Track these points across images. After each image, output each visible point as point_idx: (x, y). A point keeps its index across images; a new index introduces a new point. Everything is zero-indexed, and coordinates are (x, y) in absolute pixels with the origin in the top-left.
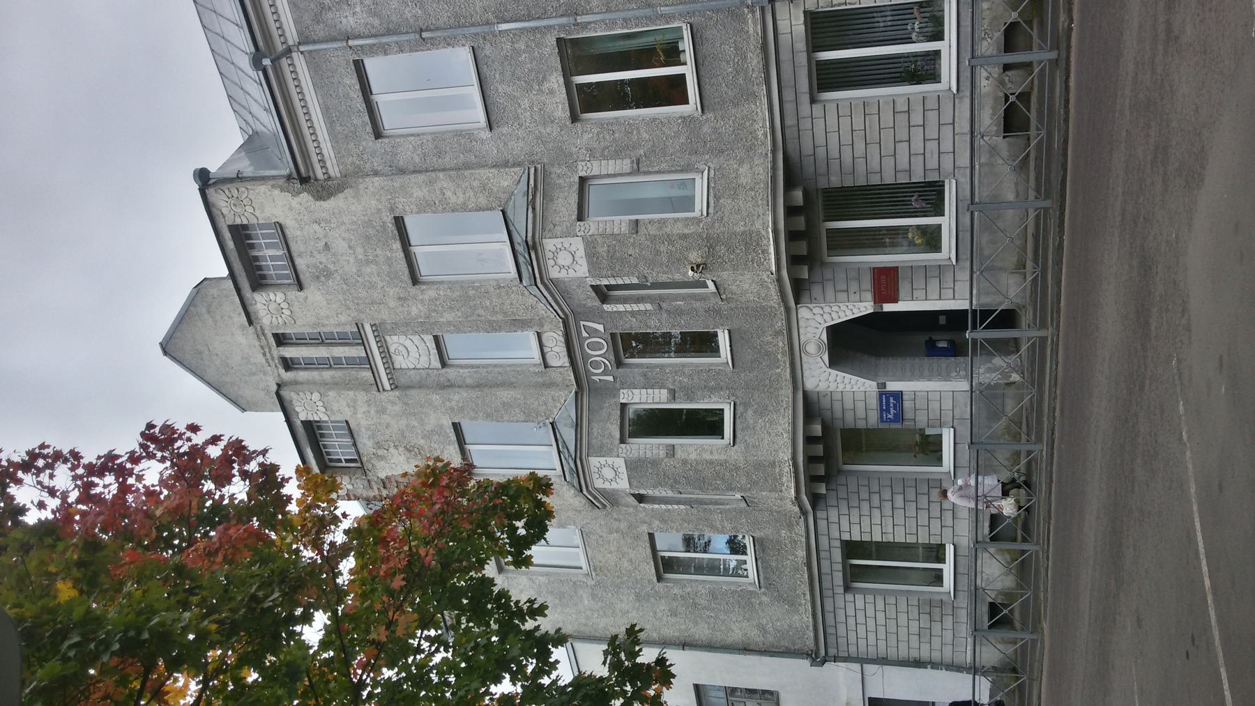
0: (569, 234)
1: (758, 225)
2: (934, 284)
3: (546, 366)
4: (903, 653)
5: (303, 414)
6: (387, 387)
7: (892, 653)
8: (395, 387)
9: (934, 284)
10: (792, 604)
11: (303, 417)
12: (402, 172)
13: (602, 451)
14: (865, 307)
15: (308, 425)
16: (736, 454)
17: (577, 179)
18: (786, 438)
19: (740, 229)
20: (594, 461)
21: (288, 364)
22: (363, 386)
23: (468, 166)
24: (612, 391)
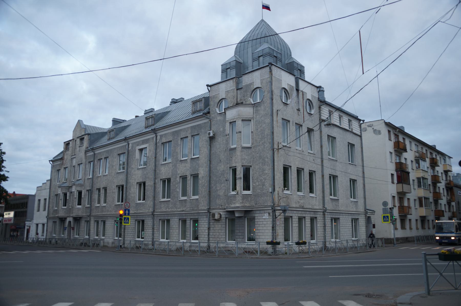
0: (75, 189)
1: (74, 214)
2: (73, 234)
3: (72, 182)
4: (48, 229)
5: (71, 143)
6: (72, 157)
7: (48, 227)
8: (72, 158)
9: (73, 234)
10: (52, 214)
11: (70, 143)
12: (86, 165)
13: (61, 190)
14: (72, 226)
15: (69, 143)
16: (60, 208)
17: (82, 190)
18: (61, 215)
19: (74, 211)
20: (60, 189)
21: (76, 141)
22: (72, 154)
23: (85, 175)
24: (69, 191)
